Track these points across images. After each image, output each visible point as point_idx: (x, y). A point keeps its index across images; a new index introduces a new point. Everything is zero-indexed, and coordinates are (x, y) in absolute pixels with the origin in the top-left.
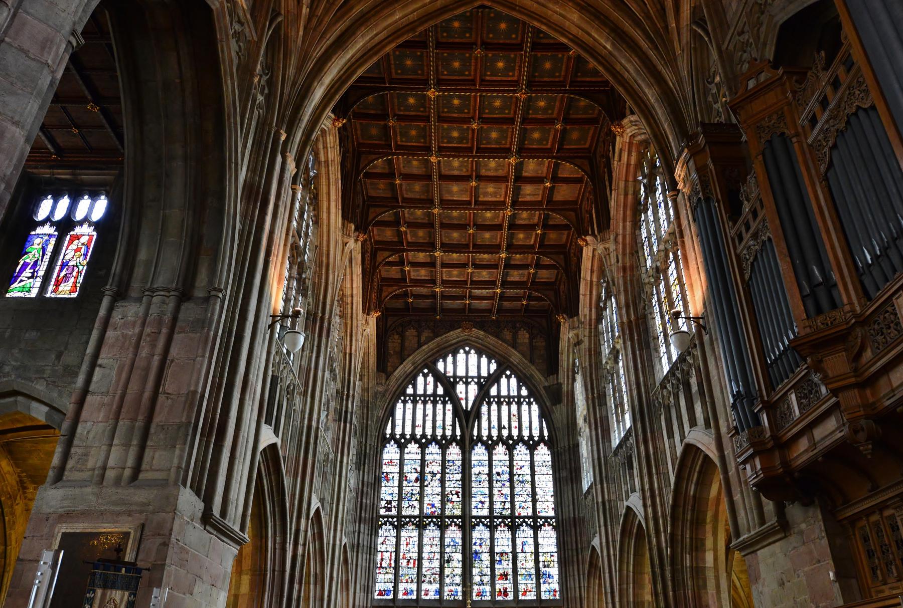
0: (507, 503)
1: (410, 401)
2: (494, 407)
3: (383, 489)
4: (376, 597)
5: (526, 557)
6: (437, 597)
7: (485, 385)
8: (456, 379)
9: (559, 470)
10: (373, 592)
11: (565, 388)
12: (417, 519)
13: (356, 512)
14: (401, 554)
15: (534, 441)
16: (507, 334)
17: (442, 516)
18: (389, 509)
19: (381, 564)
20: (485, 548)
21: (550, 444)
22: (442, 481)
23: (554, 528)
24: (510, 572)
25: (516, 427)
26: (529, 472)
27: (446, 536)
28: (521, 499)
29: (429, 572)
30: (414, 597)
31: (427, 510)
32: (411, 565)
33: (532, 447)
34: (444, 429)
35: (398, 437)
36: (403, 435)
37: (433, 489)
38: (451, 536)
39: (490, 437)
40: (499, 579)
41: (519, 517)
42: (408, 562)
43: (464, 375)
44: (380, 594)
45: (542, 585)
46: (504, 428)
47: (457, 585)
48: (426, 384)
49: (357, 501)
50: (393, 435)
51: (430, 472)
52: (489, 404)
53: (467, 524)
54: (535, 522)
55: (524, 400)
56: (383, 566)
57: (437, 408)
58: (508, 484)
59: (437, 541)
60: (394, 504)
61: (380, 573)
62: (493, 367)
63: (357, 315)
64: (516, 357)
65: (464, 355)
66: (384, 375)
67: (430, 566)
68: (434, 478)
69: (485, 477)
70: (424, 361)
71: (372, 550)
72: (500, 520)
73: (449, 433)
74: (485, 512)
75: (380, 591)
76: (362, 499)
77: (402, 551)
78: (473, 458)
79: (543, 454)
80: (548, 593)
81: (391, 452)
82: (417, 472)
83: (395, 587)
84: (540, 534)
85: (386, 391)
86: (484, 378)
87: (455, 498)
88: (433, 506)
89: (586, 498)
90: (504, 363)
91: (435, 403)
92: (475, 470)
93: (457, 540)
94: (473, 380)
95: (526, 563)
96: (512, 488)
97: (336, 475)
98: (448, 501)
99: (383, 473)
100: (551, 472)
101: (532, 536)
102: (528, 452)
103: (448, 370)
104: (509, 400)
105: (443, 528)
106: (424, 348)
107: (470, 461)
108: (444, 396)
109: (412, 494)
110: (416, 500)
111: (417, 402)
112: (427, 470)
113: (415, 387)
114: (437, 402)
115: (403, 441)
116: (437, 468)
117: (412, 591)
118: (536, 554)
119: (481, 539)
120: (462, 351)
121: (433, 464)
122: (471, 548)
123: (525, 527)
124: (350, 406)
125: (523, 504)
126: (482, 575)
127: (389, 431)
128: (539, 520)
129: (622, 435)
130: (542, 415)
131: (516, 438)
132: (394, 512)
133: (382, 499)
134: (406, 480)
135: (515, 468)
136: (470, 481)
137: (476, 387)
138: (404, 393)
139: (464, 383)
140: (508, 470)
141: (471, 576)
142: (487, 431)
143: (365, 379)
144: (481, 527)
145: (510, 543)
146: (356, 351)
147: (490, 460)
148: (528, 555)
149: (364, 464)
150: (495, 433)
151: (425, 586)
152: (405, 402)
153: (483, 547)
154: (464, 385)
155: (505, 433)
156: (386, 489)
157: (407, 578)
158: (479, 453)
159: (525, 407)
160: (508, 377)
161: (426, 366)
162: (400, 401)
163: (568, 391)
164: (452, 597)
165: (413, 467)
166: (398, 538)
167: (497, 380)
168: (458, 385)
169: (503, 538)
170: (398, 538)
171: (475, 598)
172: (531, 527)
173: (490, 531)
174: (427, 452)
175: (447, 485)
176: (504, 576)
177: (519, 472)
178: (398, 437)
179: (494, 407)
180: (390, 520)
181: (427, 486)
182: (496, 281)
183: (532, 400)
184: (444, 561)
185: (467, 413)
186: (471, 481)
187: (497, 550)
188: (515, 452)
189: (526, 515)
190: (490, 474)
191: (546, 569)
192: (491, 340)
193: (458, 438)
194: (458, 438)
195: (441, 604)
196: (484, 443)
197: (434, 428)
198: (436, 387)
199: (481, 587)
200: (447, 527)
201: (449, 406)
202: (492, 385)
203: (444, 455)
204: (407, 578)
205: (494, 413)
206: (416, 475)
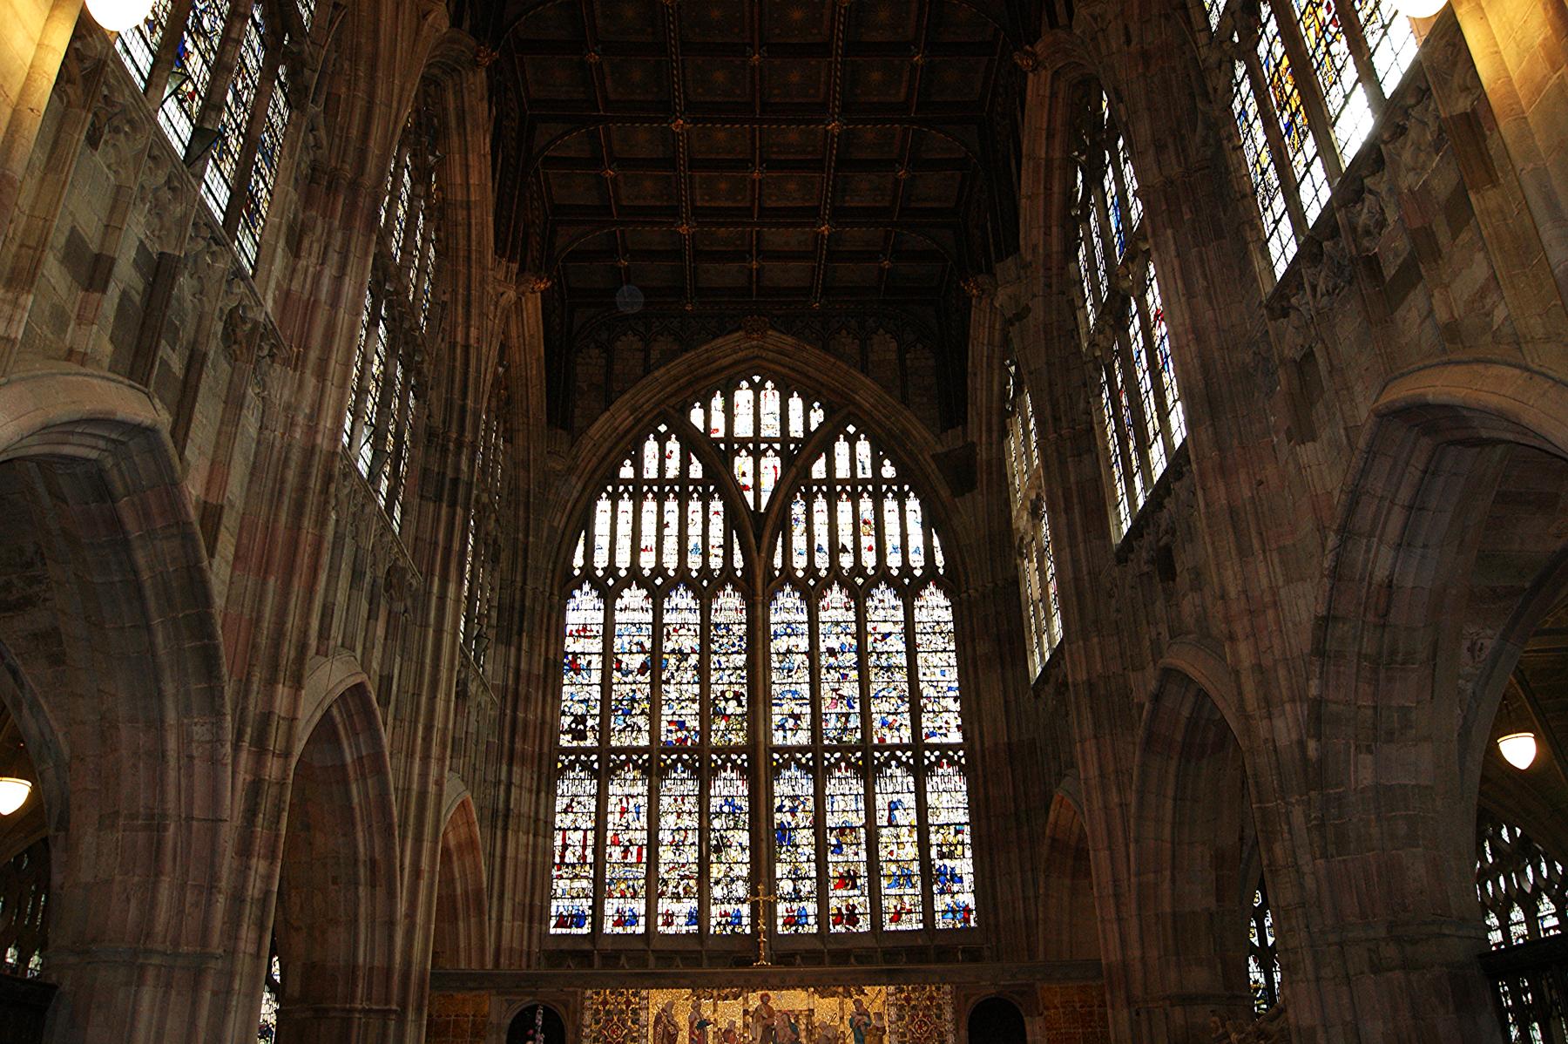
0: (852, 718)
1: (626, 495)
2: (820, 504)
3: (565, 689)
4: (552, 931)
5: (898, 836)
8: (733, 445)
9: (973, 640)
11: (982, 455)
12: (646, 757)
13: (501, 738)
14: (610, 834)
15: (912, 577)
19: (562, 857)
21: (948, 585)
22: (703, 670)
23: (964, 771)
24: (862, 870)
25: (870, 549)
26: (902, 647)
27: (712, 792)
28: (885, 707)
29: (674, 874)
30: (640, 929)
31: (668, 735)
32: (632, 859)
33: (908, 589)
34: (705, 554)
35: (600, 573)
36: (611, 569)
37: (681, 687)
38: (725, 793)
39: (811, 569)
40: (836, 887)
41: (882, 747)
42: (626, 851)
43: (751, 434)
45: (937, 898)
47: (739, 901)
48: (663, 457)
49: (503, 714)
51: (673, 652)
54: (918, 757)
55: (889, 489)
56: (567, 860)
57: (690, 509)
58: (854, 675)
59: (690, 804)
60: (590, 722)
61: (560, 877)
62: (817, 417)
63: (481, 253)
64: (867, 392)
65: (750, 393)
67: (677, 859)
68: (684, 664)
69: (799, 659)
70: (657, 405)
71: (544, 826)
72: (837, 755)
73: (716, 563)
74: (803, 738)
75: (561, 915)
76: (515, 709)
77: (610, 826)
78: (773, 619)
79: (935, 607)
80: (950, 915)
81: (584, 609)
82: (643, 651)
83: (597, 908)
86: (795, 440)
87: (732, 707)
88: (681, 725)
89: (1037, 696)
92: (780, 644)
93: (737, 802)
94: (771, 447)
95: (901, 848)
96: (864, 682)
97: (427, 625)
98: (716, 714)
99: (568, 653)
100: (952, 647)
101: (912, 789)
103: (713, 426)
104: (854, 488)
105: (704, 775)
106: (657, 374)
109: (633, 700)
110: (643, 713)
112: (669, 646)
113: (638, 466)
115: (611, 582)
116: (689, 642)
117: (635, 916)
118: (922, 828)
119: (794, 798)
120: (744, 384)
121: (682, 632)
124: (464, 467)
125: (890, 719)
126: (796, 877)
127: (578, 561)
128: (927, 753)
129: (1141, 502)
131: (870, 572)
132: (591, 741)
133: (564, 713)
134: (619, 669)
135: (870, 639)
136: (768, 667)
137: (777, 461)
138: (614, 479)
139: (749, 453)
140: (854, 642)
141: (772, 883)
142: (805, 557)
143: (520, 440)
144: (795, 772)
145: (861, 805)
146: (478, 340)
147: (813, 622)
148: (905, 830)
149: (520, 634)
150: (822, 561)
151: (664, 905)
152: (615, 498)
153: (800, 815)
154: (751, 459)
155: (846, 561)
156: (573, 689)
157: (623, 886)
158: (787, 608)
159: (890, 505)
160: (852, 440)
162: (604, 495)
163: (989, 463)
164: (729, 929)
165: (636, 639)
166: (602, 798)
168: (737, 458)
170: (602, 798)
172: (910, 770)
174: (666, 605)
175: (713, 680)
176: (848, 880)
177: (880, 647)
178: (600, 573)
179: (820, 504)
180: (583, 757)
181: (667, 682)
182: (818, 207)
183: (906, 488)
184: (710, 848)
186: (770, 670)
187: (831, 821)
189: (896, 741)
190: (813, 653)
191: (947, 862)
193: (739, 573)
194: (739, 573)
195: (702, 943)
196: (798, 585)
197: (683, 552)
198: (685, 464)
199: (795, 906)
200: (715, 772)
201: (717, 505)
203: (705, 612)
204: (623, 886)
205: (820, 519)
206: (640, 658)
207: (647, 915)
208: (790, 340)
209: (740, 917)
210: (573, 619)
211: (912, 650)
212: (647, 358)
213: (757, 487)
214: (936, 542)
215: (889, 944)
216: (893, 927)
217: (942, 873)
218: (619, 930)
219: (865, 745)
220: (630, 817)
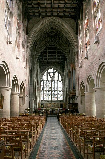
2: (55, 76)
17: (49, 90)
21: (62, 81)
22: (49, 86)
31: (47, 90)
33: (60, 82)
36: (44, 80)
37: (48, 87)
52: (55, 76)
62: (55, 71)
64: (58, 70)
71: (40, 94)
73: (49, 80)
79: (61, 82)
81: (42, 82)
91: (48, 76)
92: (53, 85)
112: (47, 85)
130: (61, 77)
132: (43, 90)
151: (47, 98)
155: (57, 80)
158: (53, 82)
159: (59, 76)
160: (57, 72)
169: (56, 92)
179: (55, 76)
185: (52, 77)
201: (50, 76)
210: (42, 83)
211: (60, 85)
219: (57, 90)
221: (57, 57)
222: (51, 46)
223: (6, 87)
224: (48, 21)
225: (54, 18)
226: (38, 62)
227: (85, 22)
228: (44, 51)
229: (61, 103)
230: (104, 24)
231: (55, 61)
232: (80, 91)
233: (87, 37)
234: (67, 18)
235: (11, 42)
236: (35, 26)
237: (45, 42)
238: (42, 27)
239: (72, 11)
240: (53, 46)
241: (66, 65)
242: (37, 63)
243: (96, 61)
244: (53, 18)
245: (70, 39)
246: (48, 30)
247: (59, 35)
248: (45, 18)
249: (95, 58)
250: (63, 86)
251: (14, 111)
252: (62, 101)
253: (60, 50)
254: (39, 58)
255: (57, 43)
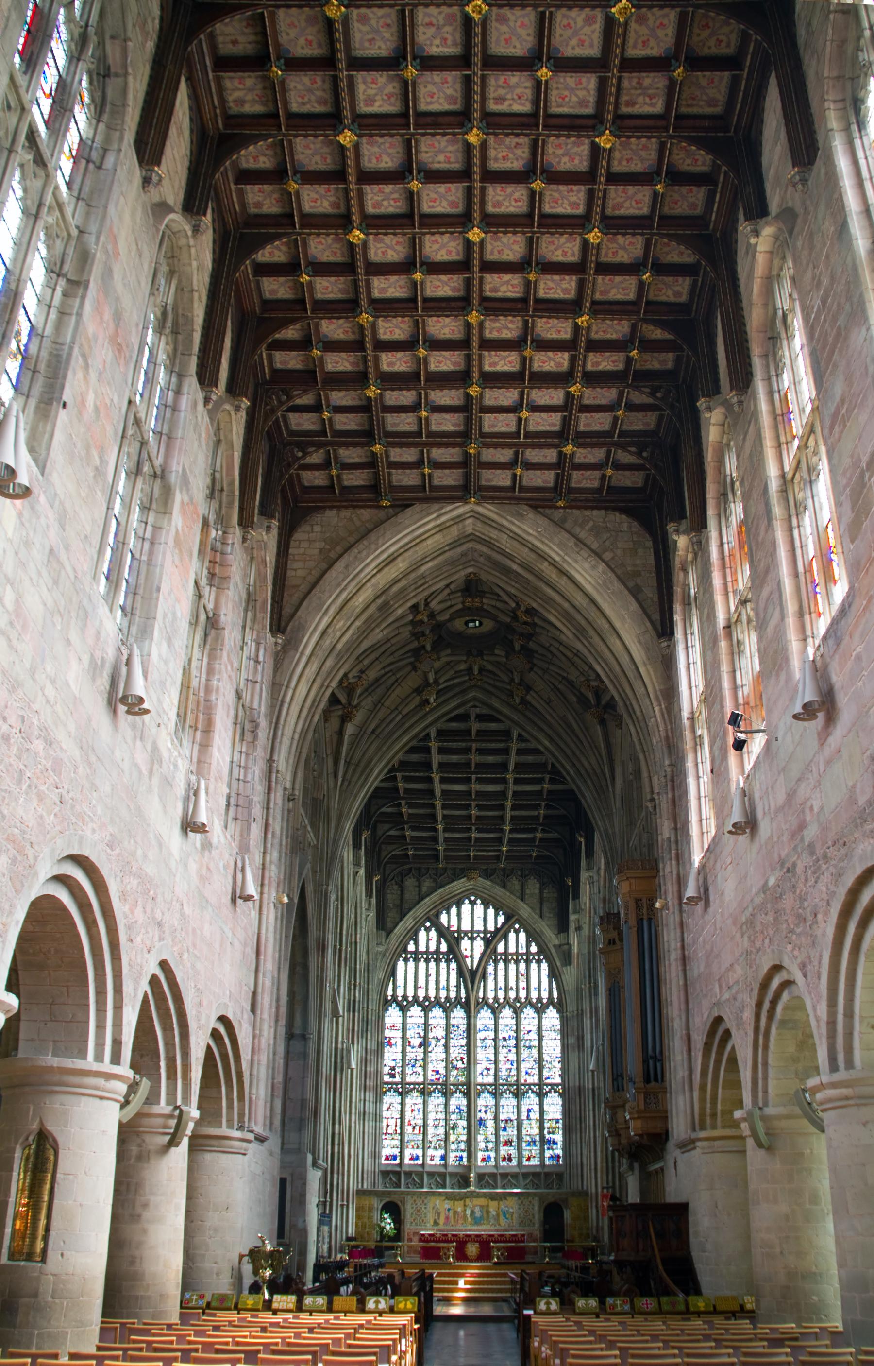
2: (501, 965)
6: (443, 1162)
7: (491, 939)
10: (380, 1157)
16: (515, 884)
17: (445, 1084)
18: (393, 1076)
20: (490, 1115)
21: (560, 1007)
22: (446, 1047)
23: (561, 1095)
24: (515, 1139)
26: (536, 1037)
31: (431, 1076)
33: (540, 1009)
34: (448, 990)
35: (400, 999)
36: (405, 997)
39: (496, 999)
44: (387, 1158)
46: (512, 989)
48: (428, 940)
50: (394, 996)
52: (496, 962)
53: (469, 1091)
54: (541, 1089)
58: (514, 1050)
59: (441, 1108)
62: (501, 919)
64: (524, 910)
66: (384, 934)
69: (490, 1043)
71: (377, 1117)
73: (453, 995)
74: (490, 1079)
78: (479, 1022)
79: (552, 1017)
81: (393, 1016)
84: (546, 1101)
85: (386, 950)
86: (491, 932)
87: (460, 1065)
88: (437, 1072)
90: (513, 916)
92: (480, 1035)
96: (518, 1054)
102: (536, 1015)
105: (447, 1094)
107: (475, 1026)
108: (447, 953)
111: (419, 960)
112: (431, 1035)
113: (416, 944)
114: (440, 960)
116: (440, 1033)
118: (541, 1121)
120: (467, 901)
122: (475, 1116)
123: (530, 1094)
130: (553, 974)
136: (476, 1046)
137: (482, 943)
138: (405, 950)
144: (486, 1095)
147: (496, 1025)
150: (501, 995)
151: (430, 1152)
152: (406, 960)
155: (512, 995)
158: (484, 1017)
159: (534, 966)
160: (517, 932)
161: (429, 919)
166: (402, 1104)
167: (506, 937)
169: (508, 1105)
170: (402, 1104)
171: (480, 1163)
173: (496, 1098)
176: (508, 1143)
177: (526, 1037)
178: (400, 999)
179: (501, 965)
185: (473, 973)
187: (502, 1117)
188: (522, 1016)
192: (499, 891)
196: (490, 1007)
197: (437, 989)
198: (439, 943)
199: (486, 1153)
200: (452, 1094)
201: (453, 965)
202: (499, 941)
203: (448, 1018)
206: (420, 1040)
207: (424, 1156)
208: (489, 883)
209: (461, 1157)
212: (420, 891)
213: (472, 957)
214: (554, 985)
215: (524, 1170)
216: (527, 1163)
217: (549, 1141)
218: (412, 1162)
219: (517, 1083)
220: (416, 1113)
221: (513, 808)
222: (464, 717)
223: (79, 1064)
224: (442, 528)
225: (487, 510)
226: (356, 846)
227: (722, 544)
228: (415, 757)
229: (552, 1193)
230: (855, 570)
231: (500, 841)
232: (702, 1100)
233: (745, 662)
234: (587, 513)
235: (141, 700)
236: (340, 565)
237: (418, 691)
238: (392, 573)
239: (625, 457)
240: (480, 718)
241: (584, 875)
242: (348, 854)
243: (819, 851)
244: (480, 509)
245: (617, 669)
246: (440, 602)
247: (530, 637)
248: (417, 507)
249: (811, 832)
250: (565, 1048)
251: (136, 1277)
252: (560, 1176)
253: (536, 752)
254: (366, 820)
255: (511, 695)
